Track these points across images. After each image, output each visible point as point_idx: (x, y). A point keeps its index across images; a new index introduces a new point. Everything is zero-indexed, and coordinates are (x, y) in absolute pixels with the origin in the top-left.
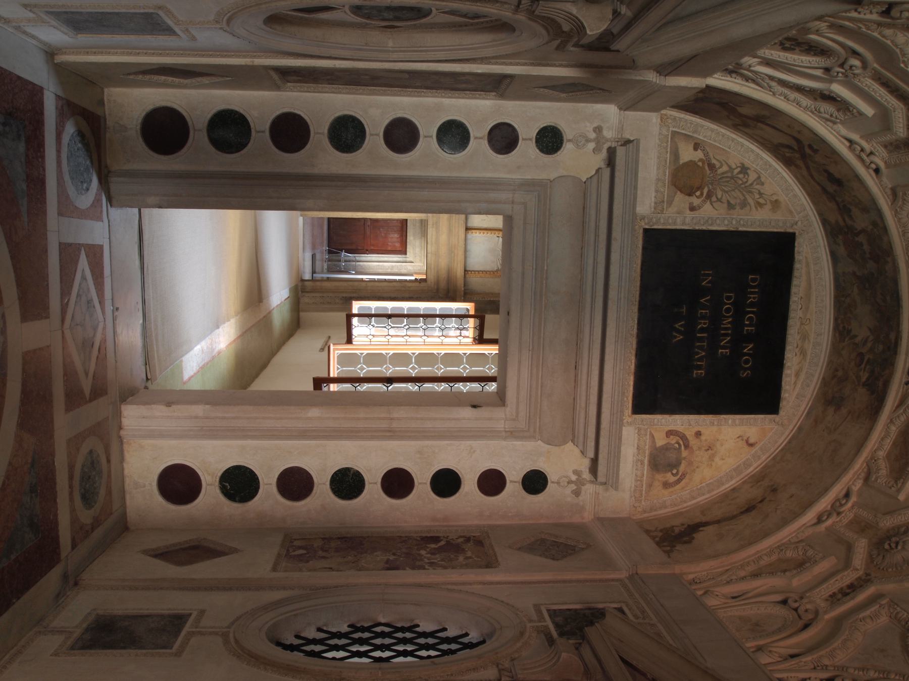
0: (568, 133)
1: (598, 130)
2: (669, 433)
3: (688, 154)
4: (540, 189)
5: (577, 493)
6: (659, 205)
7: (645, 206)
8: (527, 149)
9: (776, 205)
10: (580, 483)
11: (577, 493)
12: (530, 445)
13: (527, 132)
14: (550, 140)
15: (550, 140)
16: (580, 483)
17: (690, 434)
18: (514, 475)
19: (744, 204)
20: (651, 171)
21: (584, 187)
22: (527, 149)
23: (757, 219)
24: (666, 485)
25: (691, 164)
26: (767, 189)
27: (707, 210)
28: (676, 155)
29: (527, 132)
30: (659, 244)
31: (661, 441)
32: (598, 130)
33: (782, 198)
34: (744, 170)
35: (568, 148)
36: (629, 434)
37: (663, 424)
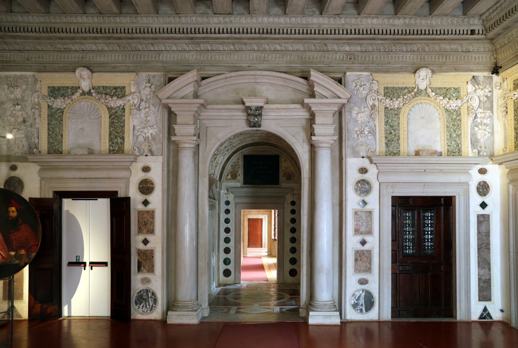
0: (226, 199)
1: (225, 194)
2: (283, 177)
3: (229, 177)
4: (236, 204)
5: (295, 195)
6: (239, 182)
7: (239, 185)
8: (229, 207)
9: (238, 159)
10: (293, 194)
11: (295, 195)
12: (286, 205)
13: (226, 207)
14: (227, 203)
15: (227, 203)
16: (293, 194)
17: (283, 173)
18: (292, 207)
19: (238, 165)
20: (233, 184)
21: (236, 197)
22: (229, 207)
23: (241, 163)
24: (294, 177)
25: (231, 176)
26: (235, 161)
27: (240, 172)
28: (230, 179)
29: (226, 207)
30: (247, 181)
31: (285, 178)
32: (225, 194)
33: (237, 158)
34: (232, 166)
35: (229, 199)
36: (284, 185)
37: (282, 178)
